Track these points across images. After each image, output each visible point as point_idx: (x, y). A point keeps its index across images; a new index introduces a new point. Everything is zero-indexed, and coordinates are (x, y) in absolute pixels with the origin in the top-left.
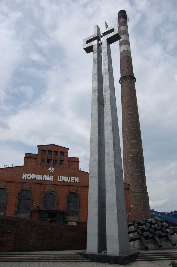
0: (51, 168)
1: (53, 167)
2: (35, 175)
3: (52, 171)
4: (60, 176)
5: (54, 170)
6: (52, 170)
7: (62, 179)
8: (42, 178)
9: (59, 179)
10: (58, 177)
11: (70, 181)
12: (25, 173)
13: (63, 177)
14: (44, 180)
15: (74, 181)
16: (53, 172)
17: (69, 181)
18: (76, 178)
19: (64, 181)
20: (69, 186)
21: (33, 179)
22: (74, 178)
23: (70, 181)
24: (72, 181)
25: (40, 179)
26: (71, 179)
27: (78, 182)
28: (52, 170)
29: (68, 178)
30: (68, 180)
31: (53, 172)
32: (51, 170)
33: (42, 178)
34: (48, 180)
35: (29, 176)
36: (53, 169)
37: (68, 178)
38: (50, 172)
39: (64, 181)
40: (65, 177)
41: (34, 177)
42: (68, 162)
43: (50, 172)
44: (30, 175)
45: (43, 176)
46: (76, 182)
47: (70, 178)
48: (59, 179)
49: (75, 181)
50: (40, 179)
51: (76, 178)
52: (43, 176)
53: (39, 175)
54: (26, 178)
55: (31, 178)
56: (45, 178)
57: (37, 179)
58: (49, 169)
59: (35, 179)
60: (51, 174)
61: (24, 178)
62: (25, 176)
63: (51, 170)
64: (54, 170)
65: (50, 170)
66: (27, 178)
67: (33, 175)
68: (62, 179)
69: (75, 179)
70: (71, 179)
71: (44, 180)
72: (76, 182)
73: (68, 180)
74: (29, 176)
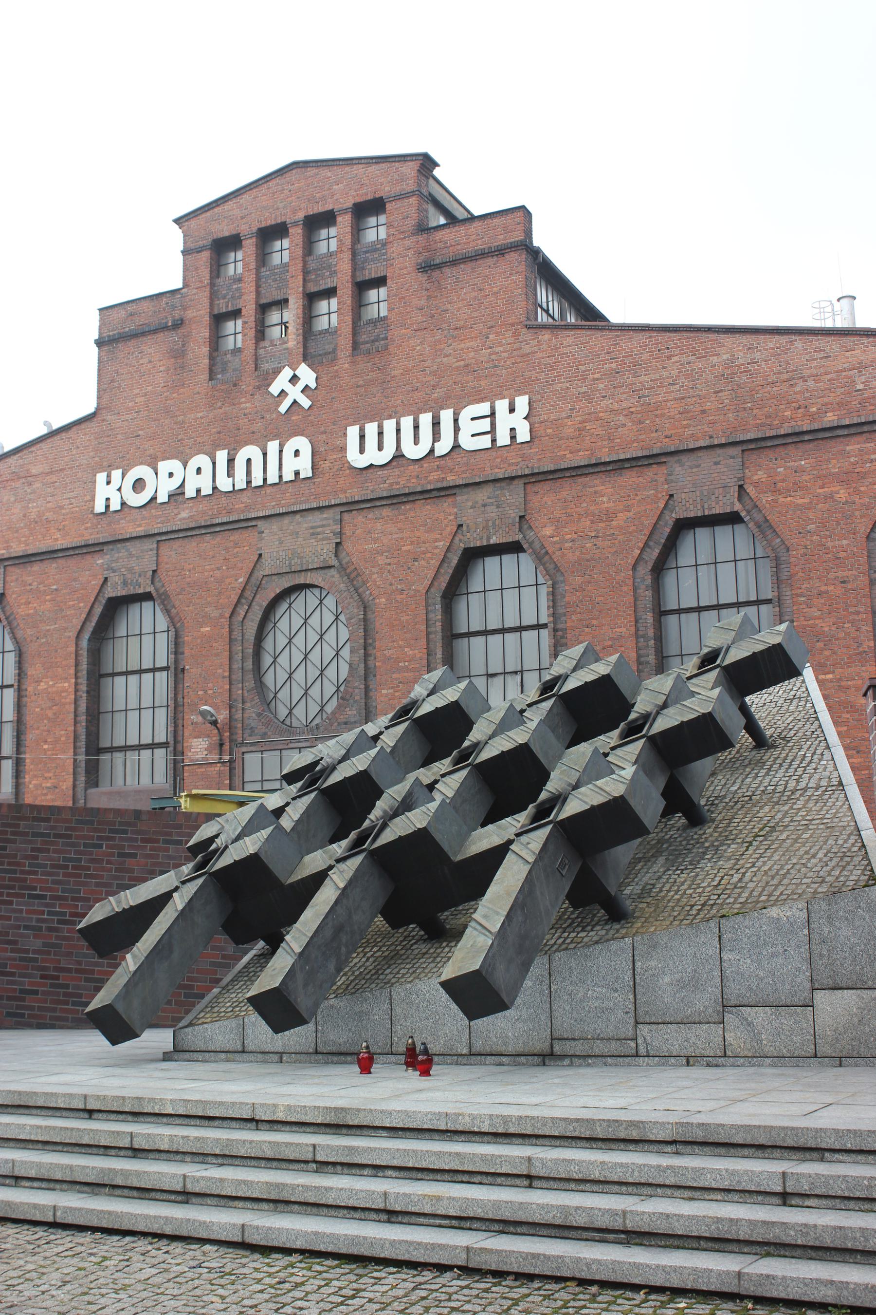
0: (287, 373)
1: (306, 358)
2: (174, 465)
3: (295, 393)
4: (361, 420)
6: (300, 385)
7: (380, 448)
8: (230, 473)
9: (362, 450)
10: (353, 432)
11: (456, 446)
12: (109, 468)
13: (389, 426)
14: (241, 484)
15: (485, 442)
16: (305, 403)
17: (444, 447)
18: (502, 406)
19: (399, 456)
20: (446, 492)
21: (162, 498)
22: (484, 408)
23: (456, 446)
24: (467, 443)
25: (215, 488)
26: (457, 429)
28: (300, 385)
29: (436, 424)
30: (436, 436)
31: (305, 403)
32: (288, 387)
33: (230, 473)
34: (273, 478)
35: (139, 485)
36: (307, 375)
37: (436, 424)
39: (399, 456)
40: (407, 422)
41: (175, 483)
42: (422, 277)
44: (141, 471)
45: (231, 461)
46: (503, 439)
47: (447, 416)
48: (362, 450)
49: (493, 431)
50: (215, 488)
51: (502, 406)
52: (231, 461)
53: (201, 460)
54: (115, 506)
55: (154, 498)
56: (249, 472)
57: (190, 492)
58: (274, 389)
59: (177, 494)
62: (111, 492)
63: (288, 387)
64: (313, 385)
68: (380, 448)
69: (493, 415)
70: (457, 429)
71: (241, 484)
72: (503, 439)
73: (436, 436)
74: (139, 485)
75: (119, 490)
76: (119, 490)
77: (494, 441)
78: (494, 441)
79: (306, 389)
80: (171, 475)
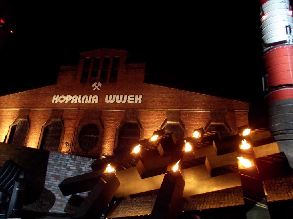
2: (70, 97)
3: (97, 87)
5: (101, 86)
6: (98, 86)
15: (132, 102)
16: (99, 89)
24: (129, 102)
26: (127, 99)
27: (140, 102)
28: (98, 86)
30: (123, 99)
31: (99, 89)
35: (62, 99)
38: (94, 89)
43: (94, 89)
46: (136, 102)
49: (134, 101)
53: (76, 96)
54: (56, 102)
58: (93, 86)
60: (95, 93)
61: (55, 102)
63: (96, 86)
64: (101, 86)
65: (94, 87)
66: (58, 102)
67: (68, 96)
69: (135, 98)
70: (127, 99)
73: (123, 99)
75: (58, 99)
76: (58, 99)
77: (134, 102)
78: (134, 102)
79: (99, 87)
80: (69, 98)
